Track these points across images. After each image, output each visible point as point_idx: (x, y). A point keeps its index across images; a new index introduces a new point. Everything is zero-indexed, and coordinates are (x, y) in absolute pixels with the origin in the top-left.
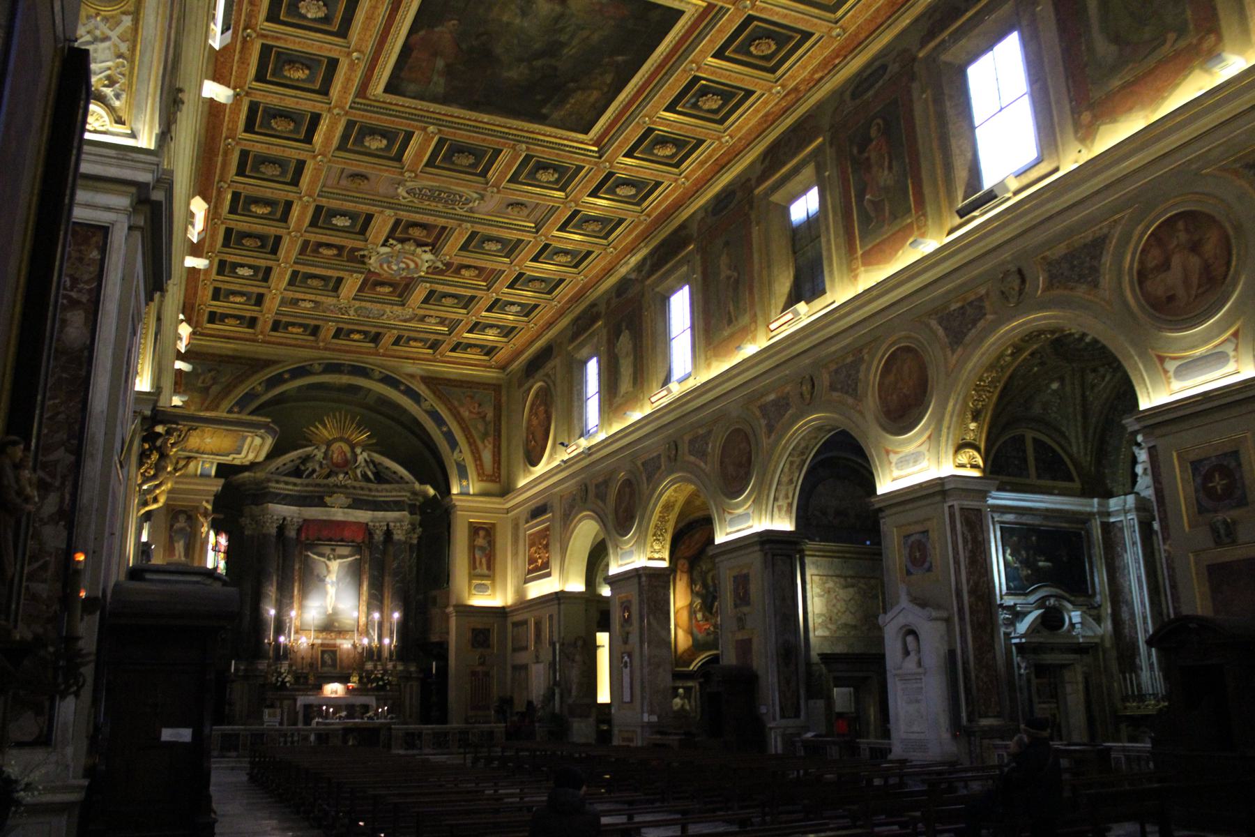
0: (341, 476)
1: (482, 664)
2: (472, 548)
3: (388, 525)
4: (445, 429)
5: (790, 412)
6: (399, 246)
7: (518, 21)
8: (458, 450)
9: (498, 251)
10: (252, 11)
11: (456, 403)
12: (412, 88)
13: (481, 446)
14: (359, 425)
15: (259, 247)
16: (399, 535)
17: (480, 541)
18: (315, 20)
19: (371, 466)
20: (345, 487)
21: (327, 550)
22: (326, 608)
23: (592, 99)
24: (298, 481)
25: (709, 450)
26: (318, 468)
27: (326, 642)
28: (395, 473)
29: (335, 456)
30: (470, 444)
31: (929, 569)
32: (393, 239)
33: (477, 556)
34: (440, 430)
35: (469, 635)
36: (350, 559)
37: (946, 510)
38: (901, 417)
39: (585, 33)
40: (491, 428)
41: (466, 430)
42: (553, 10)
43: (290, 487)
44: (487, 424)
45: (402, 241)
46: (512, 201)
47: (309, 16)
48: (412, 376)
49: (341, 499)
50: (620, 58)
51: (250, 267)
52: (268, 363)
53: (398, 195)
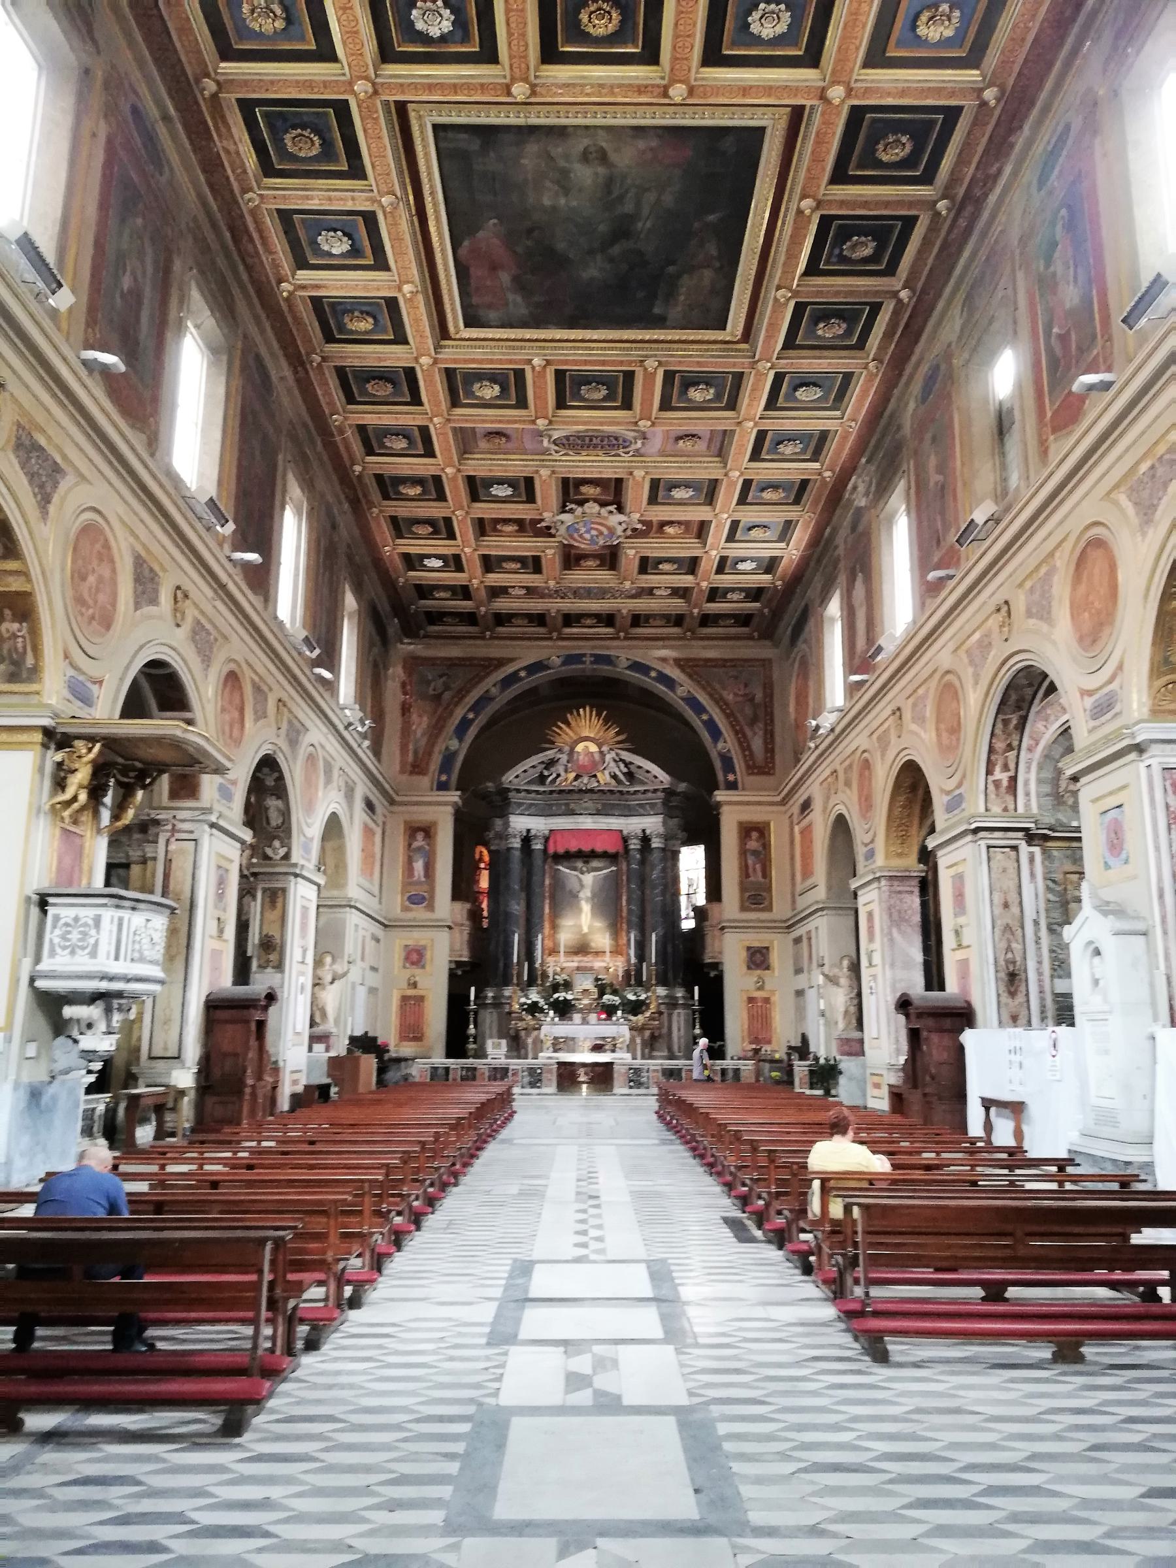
0: (585, 780)
1: (761, 988)
2: (743, 853)
5: (992, 653)
6: (579, 510)
7: (562, 201)
8: (721, 740)
9: (691, 497)
10: (273, 260)
11: (717, 686)
12: (493, 315)
13: (749, 733)
14: (606, 721)
15: (431, 533)
16: (656, 843)
17: (753, 844)
18: (343, 255)
19: (622, 765)
20: (591, 791)
21: (580, 864)
22: (580, 927)
23: (707, 282)
24: (541, 789)
25: (928, 714)
26: (563, 774)
27: (582, 964)
28: (648, 772)
29: (581, 758)
30: (736, 733)
31: (1126, 862)
32: (572, 502)
33: (750, 862)
35: (744, 954)
37: (1143, 771)
38: (1094, 641)
39: (651, 197)
40: (761, 713)
41: (730, 716)
42: (596, 174)
43: (533, 795)
45: (581, 503)
46: (681, 434)
47: (335, 251)
48: (664, 660)
49: (588, 803)
50: (711, 218)
51: (438, 557)
52: (501, 662)
53: (548, 449)
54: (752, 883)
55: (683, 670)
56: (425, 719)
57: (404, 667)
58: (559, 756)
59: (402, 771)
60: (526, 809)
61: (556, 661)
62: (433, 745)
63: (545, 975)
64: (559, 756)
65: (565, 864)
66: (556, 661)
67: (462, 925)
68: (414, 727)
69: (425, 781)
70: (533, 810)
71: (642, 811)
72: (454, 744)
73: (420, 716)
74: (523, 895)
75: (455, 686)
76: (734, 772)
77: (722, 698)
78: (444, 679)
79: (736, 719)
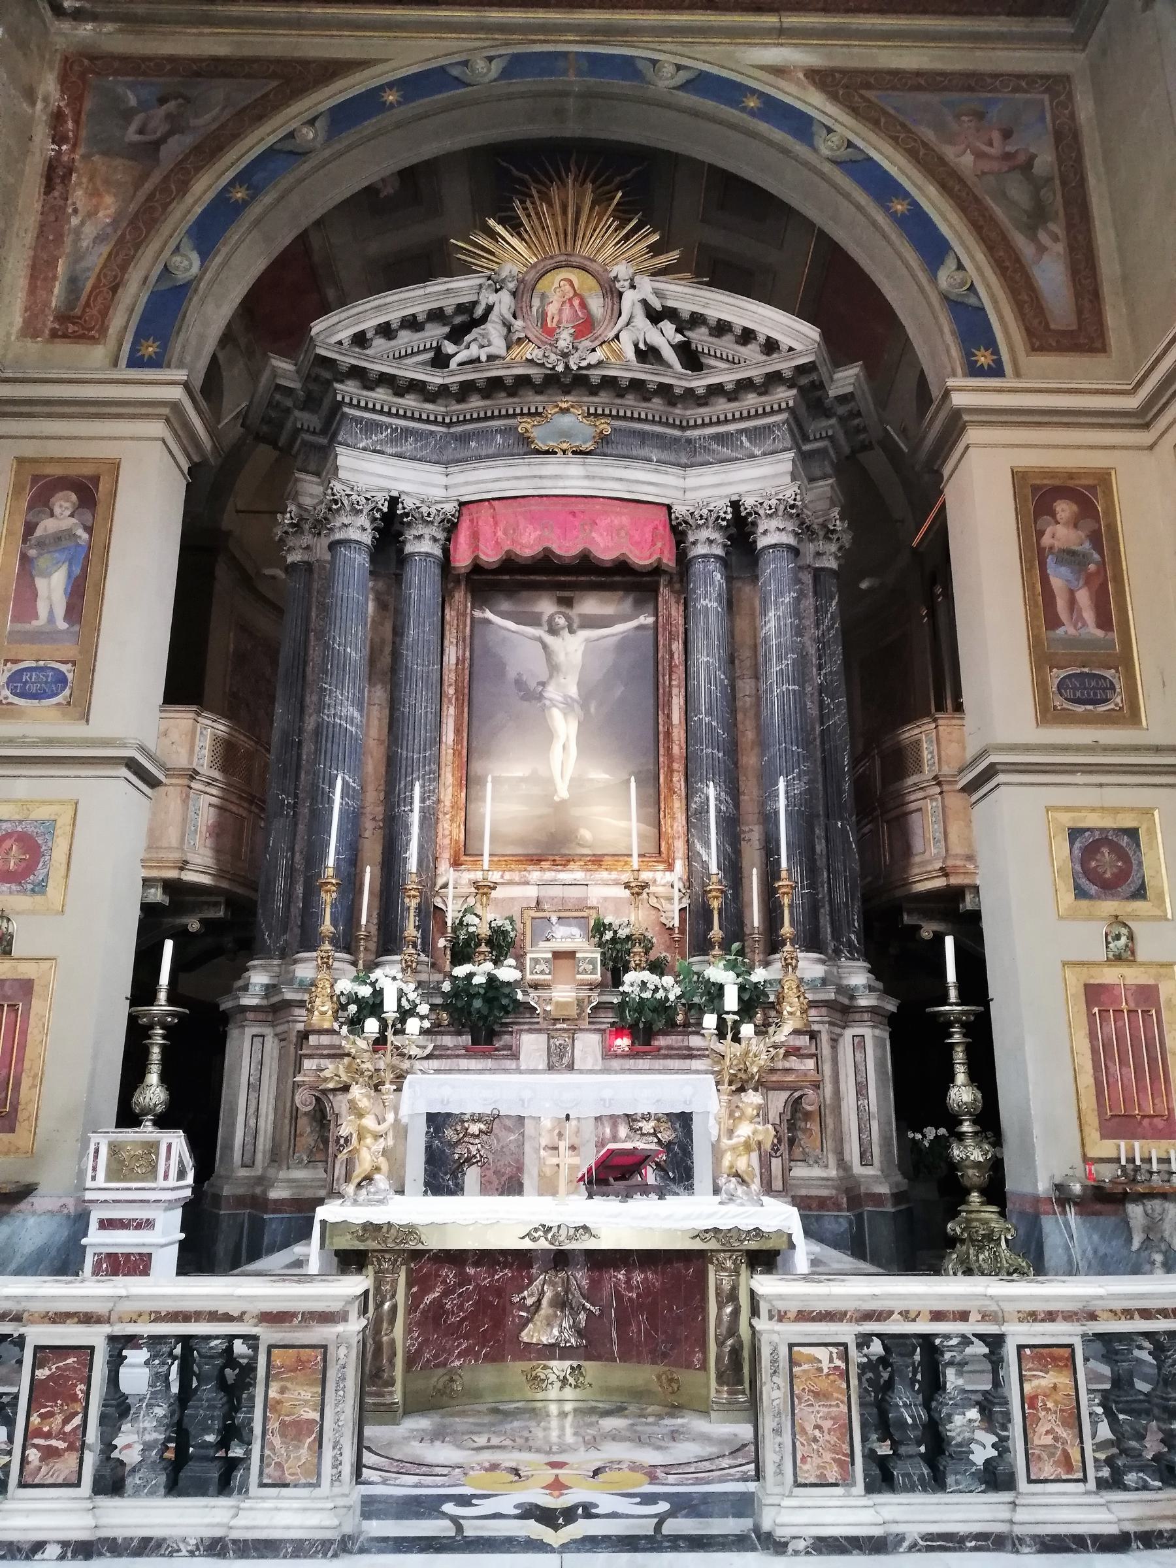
3: (735, 505)
4: (900, 207)
8: (951, 264)
21: (546, 607)
22: (550, 781)
30: (990, 248)
34: (887, 210)
36: (620, 628)
40: (1055, 199)
44: (1036, 185)
54: (1071, 642)
55: (834, 97)
56: (109, 200)
57: (63, 80)
58: (488, 297)
59: (30, 330)
60: (391, 440)
61: (485, 71)
62: (124, 267)
63: (431, 915)
64: (488, 297)
65: (506, 606)
66: (485, 71)
67: (193, 775)
68: (75, 221)
69: (98, 354)
70: (408, 446)
71: (725, 451)
72: (188, 264)
73: (94, 193)
74: (380, 694)
75: (205, 121)
76: (991, 344)
77: (942, 161)
78: (171, 106)
79: (984, 210)
